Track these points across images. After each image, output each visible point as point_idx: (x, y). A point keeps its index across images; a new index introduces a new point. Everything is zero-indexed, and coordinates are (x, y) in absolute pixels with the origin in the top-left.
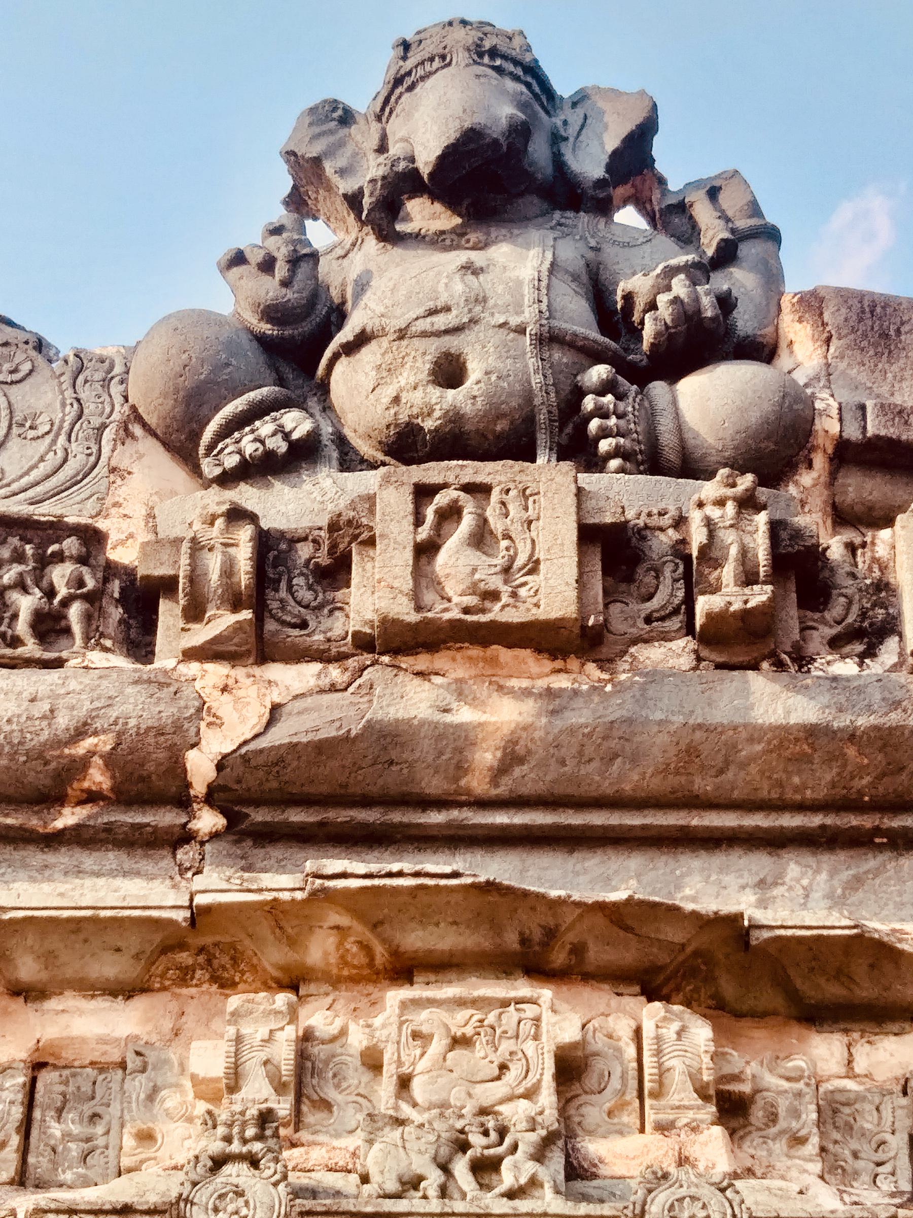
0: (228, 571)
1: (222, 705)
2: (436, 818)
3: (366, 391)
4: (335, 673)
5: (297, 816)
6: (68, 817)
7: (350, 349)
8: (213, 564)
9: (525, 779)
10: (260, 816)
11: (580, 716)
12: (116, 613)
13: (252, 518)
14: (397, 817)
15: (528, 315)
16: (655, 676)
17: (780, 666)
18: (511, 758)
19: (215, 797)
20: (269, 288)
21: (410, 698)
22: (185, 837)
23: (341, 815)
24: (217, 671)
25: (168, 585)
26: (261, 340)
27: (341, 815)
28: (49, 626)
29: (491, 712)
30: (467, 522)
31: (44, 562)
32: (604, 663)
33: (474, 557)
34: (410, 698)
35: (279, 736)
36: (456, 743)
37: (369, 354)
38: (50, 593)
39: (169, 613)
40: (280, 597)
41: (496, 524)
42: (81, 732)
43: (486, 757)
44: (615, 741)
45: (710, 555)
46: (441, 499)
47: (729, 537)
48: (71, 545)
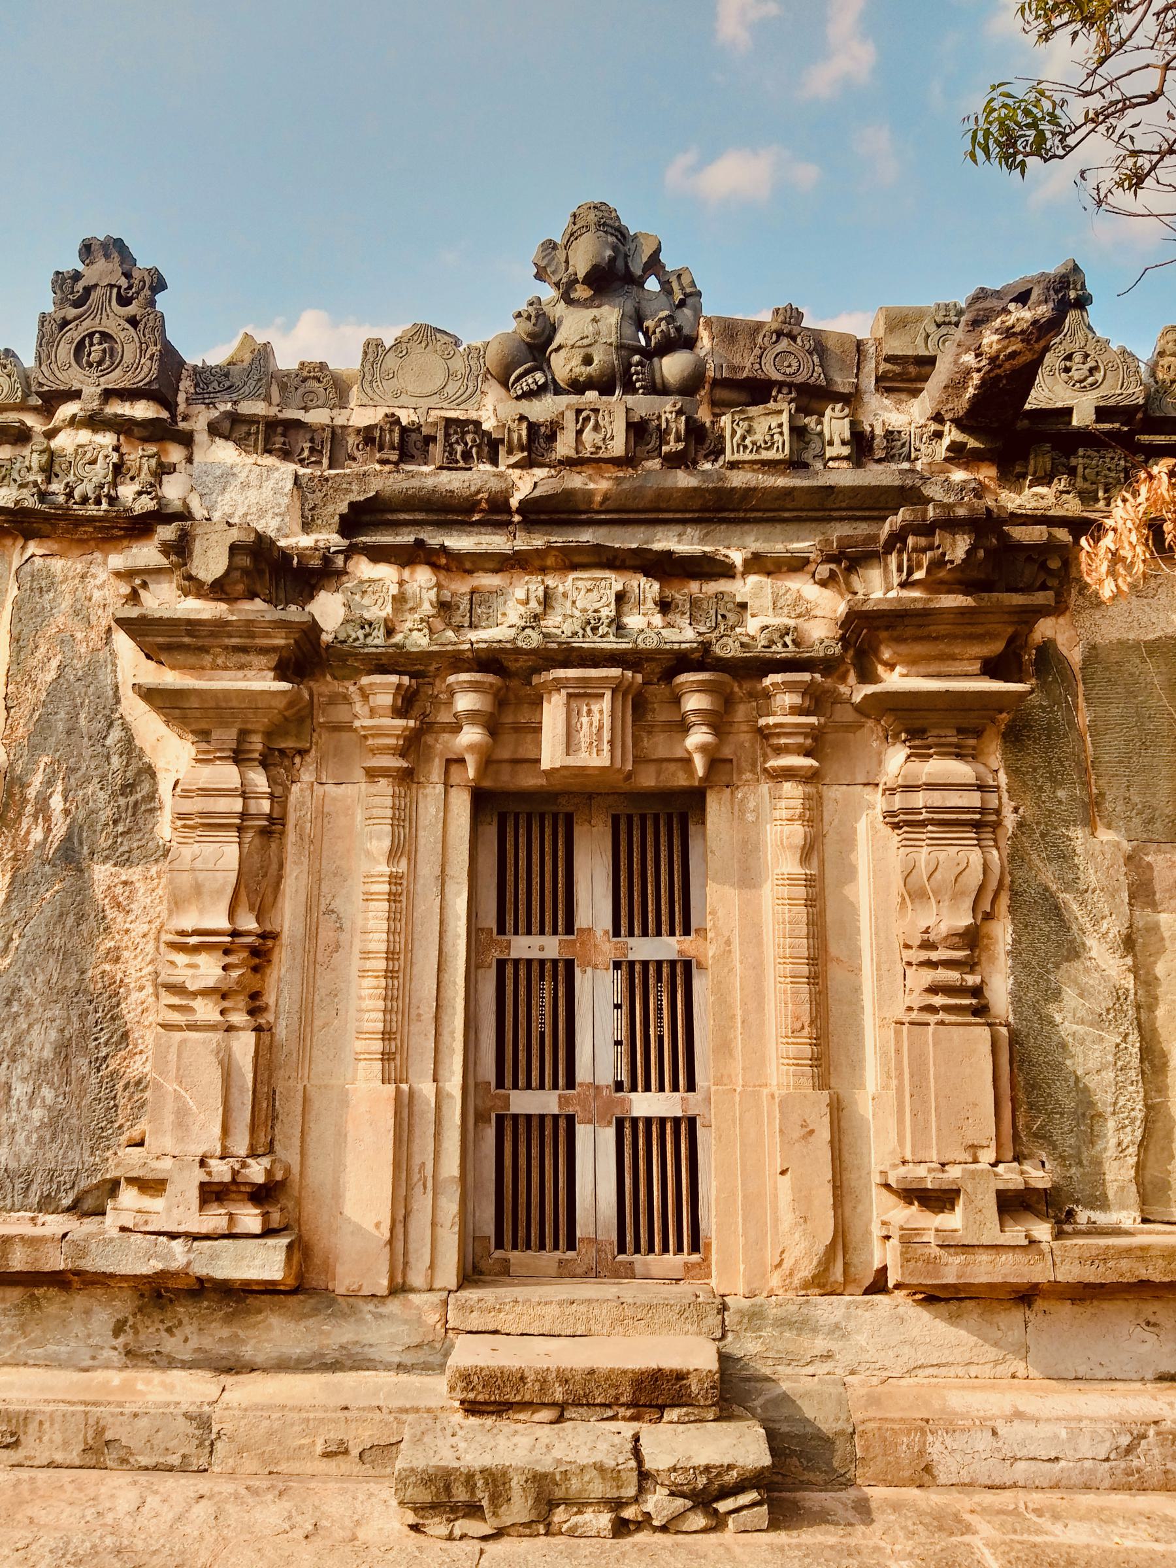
0: (520, 436)
1: (519, 483)
2: (584, 517)
3: (563, 365)
4: (553, 472)
5: (543, 517)
6: (476, 517)
7: (557, 350)
8: (515, 436)
9: (610, 504)
10: (532, 517)
11: (626, 486)
12: (486, 449)
13: (526, 418)
14: (572, 517)
15: (613, 339)
16: (649, 472)
17: (687, 467)
18: (606, 498)
19: (518, 511)
20: (529, 326)
21: (576, 481)
22: (511, 523)
23: (556, 516)
24: (518, 472)
25: (502, 441)
26: (527, 344)
27: (556, 516)
28: (467, 456)
29: (600, 485)
30: (592, 422)
31: (464, 433)
32: (634, 468)
33: (594, 435)
34: (576, 481)
35: (537, 493)
36: (590, 494)
37: (562, 353)
38: (466, 444)
39: (502, 451)
40: (537, 443)
41: (601, 423)
42: (478, 492)
43: (598, 499)
44: (637, 492)
45: (667, 431)
46: (584, 414)
47: (673, 425)
48: (471, 427)
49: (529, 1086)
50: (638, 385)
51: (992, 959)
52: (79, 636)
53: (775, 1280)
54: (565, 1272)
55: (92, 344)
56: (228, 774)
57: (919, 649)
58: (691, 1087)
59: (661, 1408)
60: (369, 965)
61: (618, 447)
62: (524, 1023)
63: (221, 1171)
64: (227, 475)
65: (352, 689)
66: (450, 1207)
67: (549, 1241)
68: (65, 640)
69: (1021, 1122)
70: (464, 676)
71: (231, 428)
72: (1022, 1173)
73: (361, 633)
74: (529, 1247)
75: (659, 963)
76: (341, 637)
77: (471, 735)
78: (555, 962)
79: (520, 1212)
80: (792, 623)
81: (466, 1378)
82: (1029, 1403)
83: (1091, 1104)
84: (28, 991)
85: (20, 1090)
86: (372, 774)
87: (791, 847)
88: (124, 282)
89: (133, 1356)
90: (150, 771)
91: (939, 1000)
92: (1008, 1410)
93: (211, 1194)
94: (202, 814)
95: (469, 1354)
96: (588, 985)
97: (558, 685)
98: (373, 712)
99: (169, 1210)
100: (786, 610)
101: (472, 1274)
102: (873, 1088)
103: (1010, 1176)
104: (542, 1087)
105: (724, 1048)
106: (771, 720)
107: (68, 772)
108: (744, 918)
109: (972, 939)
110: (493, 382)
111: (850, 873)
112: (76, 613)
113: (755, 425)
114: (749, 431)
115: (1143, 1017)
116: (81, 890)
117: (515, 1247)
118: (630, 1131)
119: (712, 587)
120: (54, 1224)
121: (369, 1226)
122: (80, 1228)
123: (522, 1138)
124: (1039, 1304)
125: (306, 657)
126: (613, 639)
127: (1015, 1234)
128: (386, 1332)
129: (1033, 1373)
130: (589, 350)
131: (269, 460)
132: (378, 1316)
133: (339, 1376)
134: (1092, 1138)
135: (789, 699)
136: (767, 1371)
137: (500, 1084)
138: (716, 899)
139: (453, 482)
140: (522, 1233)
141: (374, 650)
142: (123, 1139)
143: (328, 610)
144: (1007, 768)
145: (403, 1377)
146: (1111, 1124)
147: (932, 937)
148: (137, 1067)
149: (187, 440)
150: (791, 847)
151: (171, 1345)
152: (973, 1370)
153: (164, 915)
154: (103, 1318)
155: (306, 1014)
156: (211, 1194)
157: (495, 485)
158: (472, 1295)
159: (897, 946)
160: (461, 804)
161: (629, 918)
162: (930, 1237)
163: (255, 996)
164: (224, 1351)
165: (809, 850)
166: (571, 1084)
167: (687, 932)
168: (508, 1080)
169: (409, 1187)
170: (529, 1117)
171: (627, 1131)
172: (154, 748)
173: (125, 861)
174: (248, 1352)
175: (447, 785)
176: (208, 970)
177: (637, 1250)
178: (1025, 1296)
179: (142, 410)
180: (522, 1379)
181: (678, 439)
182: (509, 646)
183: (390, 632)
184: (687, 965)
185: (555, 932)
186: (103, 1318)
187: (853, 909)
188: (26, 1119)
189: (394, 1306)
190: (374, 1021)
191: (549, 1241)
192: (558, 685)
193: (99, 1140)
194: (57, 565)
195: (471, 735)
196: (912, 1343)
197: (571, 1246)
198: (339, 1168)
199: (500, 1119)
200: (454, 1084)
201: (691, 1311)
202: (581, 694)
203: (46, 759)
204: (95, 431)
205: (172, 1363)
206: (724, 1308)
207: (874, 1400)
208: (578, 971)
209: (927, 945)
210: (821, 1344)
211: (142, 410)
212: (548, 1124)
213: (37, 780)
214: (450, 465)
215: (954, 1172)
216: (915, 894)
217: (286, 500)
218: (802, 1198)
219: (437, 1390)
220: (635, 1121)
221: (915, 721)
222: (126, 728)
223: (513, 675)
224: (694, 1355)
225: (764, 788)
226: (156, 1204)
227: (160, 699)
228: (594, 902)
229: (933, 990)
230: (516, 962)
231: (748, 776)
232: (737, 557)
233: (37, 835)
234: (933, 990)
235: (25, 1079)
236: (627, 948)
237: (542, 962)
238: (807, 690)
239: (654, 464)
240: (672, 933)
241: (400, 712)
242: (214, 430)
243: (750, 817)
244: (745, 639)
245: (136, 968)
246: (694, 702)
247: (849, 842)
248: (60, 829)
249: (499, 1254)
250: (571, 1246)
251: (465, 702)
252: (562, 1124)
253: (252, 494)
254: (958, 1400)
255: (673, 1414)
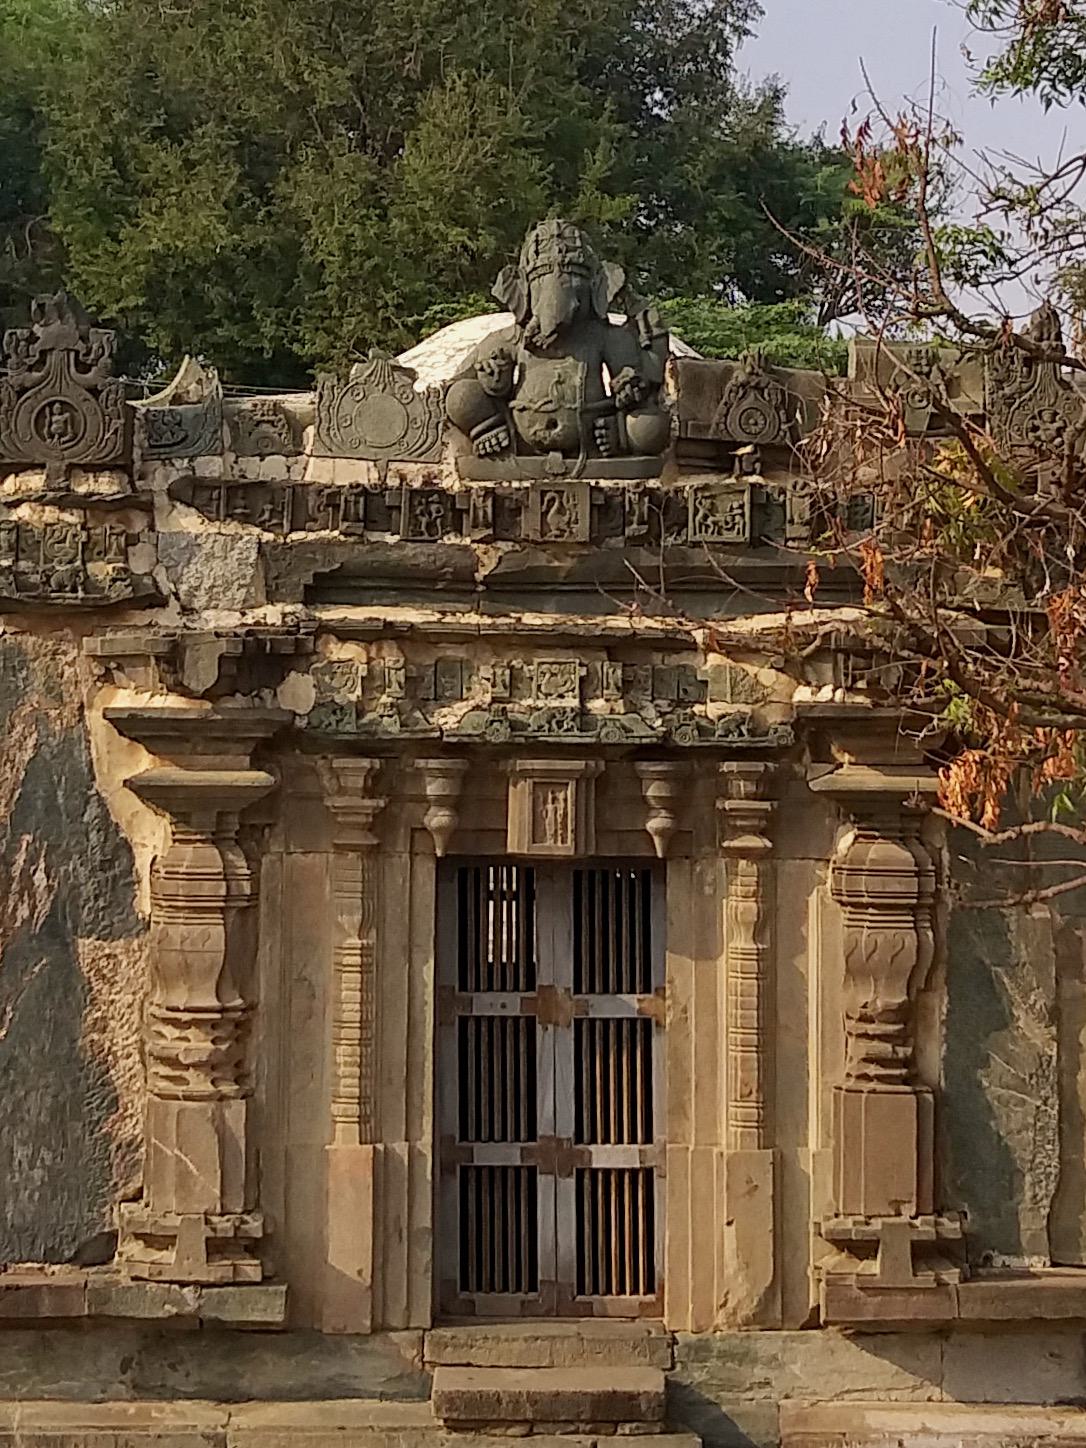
2: (548, 587)
4: (517, 547)
21: (542, 559)
22: (475, 591)
24: (483, 546)
28: (430, 526)
30: (556, 504)
31: (428, 503)
39: (467, 522)
43: (563, 574)
49: (491, 1138)
50: (602, 448)
51: (929, 1028)
52: (53, 713)
53: (720, 1318)
54: (526, 1312)
55: (52, 414)
56: (210, 857)
57: (864, 742)
58: (648, 1139)
59: (616, 1423)
60: (344, 1033)
61: (582, 530)
62: (485, 1073)
63: (224, 1225)
64: (193, 545)
65: (321, 762)
66: (425, 1256)
67: (512, 1285)
68: (39, 719)
69: (946, 1179)
70: (433, 763)
71: (193, 492)
72: (937, 1224)
73: (333, 719)
74: (492, 1289)
75: (619, 1021)
76: (315, 722)
77: (437, 818)
78: (516, 1019)
79: (483, 1255)
80: (747, 709)
81: (450, 1400)
82: (936, 1422)
83: (1012, 1162)
84: (23, 1060)
85: (20, 1153)
86: (340, 849)
87: (745, 923)
88: (81, 346)
89: (141, 1391)
90: (127, 847)
91: (873, 1070)
92: (917, 1427)
93: (216, 1248)
94: (189, 898)
95: (444, 1381)
96: (549, 1040)
97: (525, 774)
98: (342, 791)
99: (179, 1260)
100: (743, 696)
101: (442, 1316)
102: (814, 1143)
103: (925, 1227)
104: (504, 1138)
105: (678, 1110)
106: (728, 805)
107: (55, 855)
108: (704, 995)
109: (908, 1017)
110: (453, 429)
111: (801, 945)
112: (50, 690)
113: (717, 502)
114: (712, 510)
115: (1065, 1080)
116: (67, 962)
117: (479, 1288)
118: (593, 1185)
119: (674, 660)
120: (60, 1274)
121: (351, 1273)
122: (93, 1276)
123: (485, 1187)
124: (955, 1338)
125: (277, 743)
126: (576, 732)
127: (926, 1278)
128: (368, 1368)
129: (946, 1397)
130: (553, 415)
131: (232, 528)
132: (361, 1352)
133: (328, 1404)
134: (1012, 1191)
135: (743, 786)
136: (711, 1397)
137: (464, 1137)
138: (678, 970)
139: (416, 554)
140: (486, 1275)
141: (346, 737)
142: (118, 1195)
143: (299, 693)
144: (949, 846)
145: (386, 1404)
146: (1028, 1179)
147: (869, 1011)
148: (128, 1130)
149: (148, 508)
150: (745, 923)
151: (175, 1379)
152: (894, 1395)
153: (148, 987)
154: (110, 1358)
155: (283, 1076)
156: (216, 1248)
157: (462, 561)
158: (446, 1333)
159: (842, 1014)
160: (426, 873)
161: (591, 975)
162: (852, 1281)
163: (238, 1065)
164: (223, 1383)
165: (760, 928)
166: (532, 1135)
167: (647, 989)
168: (472, 1134)
169: (387, 1238)
170: (491, 1169)
171: (587, 1181)
172: (130, 823)
173: (108, 936)
174: (244, 1384)
175: (413, 854)
176: (200, 1045)
177: (596, 1291)
178: (942, 1331)
179: (105, 485)
180: (499, 1401)
181: (641, 522)
182: (477, 739)
183: (360, 714)
184: (647, 1023)
185: (516, 988)
186: (110, 1358)
187: (803, 979)
188: (29, 1179)
189: (376, 1344)
190: (349, 1086)
191: (512, 1285)
192: (525, 774)
193: (98, 1196)
194: (30, 641)
195: (437, 818)
196: (841, 1372)
197: (533, 1287)
198: (322, 1220)
199: (464, 1170)
200: (425, 1143)
201: (645, 1346)
202: (546, 784)
203: (28, 838)
204: (62, 510)
205: (175, 1396)
206: (675, 1341)
207: (801, 1418)
208: (539, 1027)
209: (863, 1019)
210: (759, 1373)
211: (105, 485)
212: (511, 1174)
213: (21, 859)
214: (414, 535)
215: (877, 1224)
216: (857, 970)
217: (250, 571)
218: (744, 1247)
219: (425, 1413)
220: (594, 1172)
221: (864, 810)
222: (102, 803)
223: (479, 764)
224: (648, 1381)
225: (722, 863)
226: (169, 1256)
227: (147, 791)
228: (556, 964)
229: (868, 1060)
230: (478, 1019)
231: (707, 849)
232: (699, 636)
233: (24, 912)
234: (868, 1060)
235: (24, 1144)
236: (585, 1007)
237: (504, 1019)
238: (759, 779)
239: (618, 542)
240: (632, 991)
241: (369, 792)
242: (173, 494)
243: (708, 890)
244: (704, 723)
245: (122, 1038)
246: (653, 791)
247: (802, 916)
248: (43, 908)
249: (464, 1295)
250: (533, 1287)
251: (433, 789)
252: (524, 1174)
253: (216, 564)
254: (873, 1419)
255: (627, 1429)
